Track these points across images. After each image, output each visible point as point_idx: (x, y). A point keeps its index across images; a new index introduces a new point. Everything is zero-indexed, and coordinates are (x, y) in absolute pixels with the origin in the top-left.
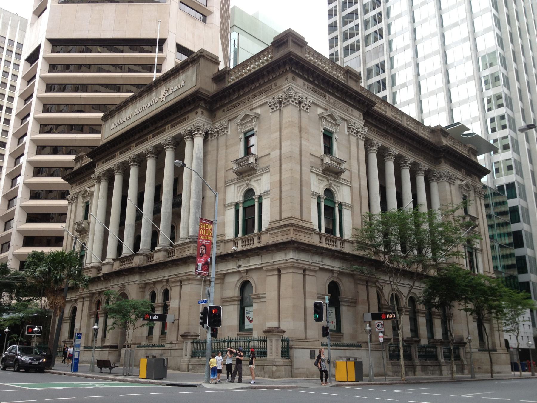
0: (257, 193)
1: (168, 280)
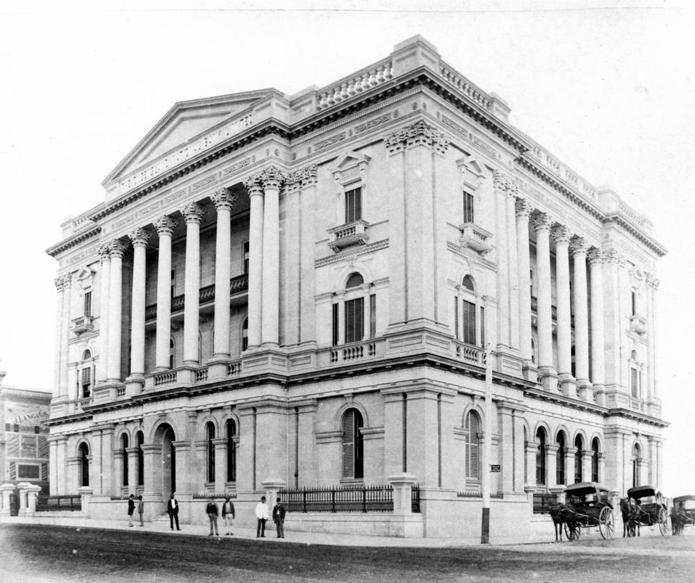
0: (367, 280)
1: (233, 407)
